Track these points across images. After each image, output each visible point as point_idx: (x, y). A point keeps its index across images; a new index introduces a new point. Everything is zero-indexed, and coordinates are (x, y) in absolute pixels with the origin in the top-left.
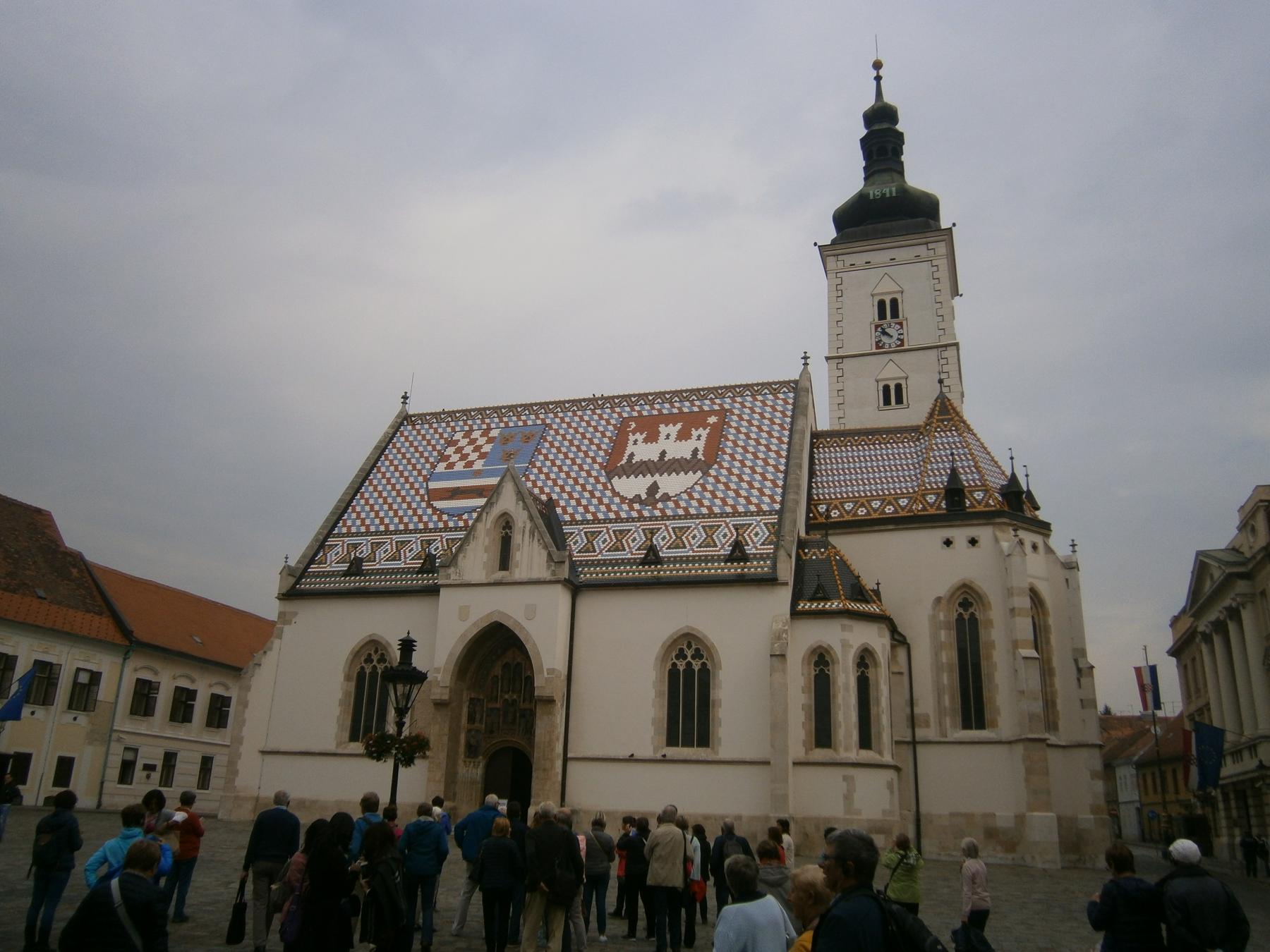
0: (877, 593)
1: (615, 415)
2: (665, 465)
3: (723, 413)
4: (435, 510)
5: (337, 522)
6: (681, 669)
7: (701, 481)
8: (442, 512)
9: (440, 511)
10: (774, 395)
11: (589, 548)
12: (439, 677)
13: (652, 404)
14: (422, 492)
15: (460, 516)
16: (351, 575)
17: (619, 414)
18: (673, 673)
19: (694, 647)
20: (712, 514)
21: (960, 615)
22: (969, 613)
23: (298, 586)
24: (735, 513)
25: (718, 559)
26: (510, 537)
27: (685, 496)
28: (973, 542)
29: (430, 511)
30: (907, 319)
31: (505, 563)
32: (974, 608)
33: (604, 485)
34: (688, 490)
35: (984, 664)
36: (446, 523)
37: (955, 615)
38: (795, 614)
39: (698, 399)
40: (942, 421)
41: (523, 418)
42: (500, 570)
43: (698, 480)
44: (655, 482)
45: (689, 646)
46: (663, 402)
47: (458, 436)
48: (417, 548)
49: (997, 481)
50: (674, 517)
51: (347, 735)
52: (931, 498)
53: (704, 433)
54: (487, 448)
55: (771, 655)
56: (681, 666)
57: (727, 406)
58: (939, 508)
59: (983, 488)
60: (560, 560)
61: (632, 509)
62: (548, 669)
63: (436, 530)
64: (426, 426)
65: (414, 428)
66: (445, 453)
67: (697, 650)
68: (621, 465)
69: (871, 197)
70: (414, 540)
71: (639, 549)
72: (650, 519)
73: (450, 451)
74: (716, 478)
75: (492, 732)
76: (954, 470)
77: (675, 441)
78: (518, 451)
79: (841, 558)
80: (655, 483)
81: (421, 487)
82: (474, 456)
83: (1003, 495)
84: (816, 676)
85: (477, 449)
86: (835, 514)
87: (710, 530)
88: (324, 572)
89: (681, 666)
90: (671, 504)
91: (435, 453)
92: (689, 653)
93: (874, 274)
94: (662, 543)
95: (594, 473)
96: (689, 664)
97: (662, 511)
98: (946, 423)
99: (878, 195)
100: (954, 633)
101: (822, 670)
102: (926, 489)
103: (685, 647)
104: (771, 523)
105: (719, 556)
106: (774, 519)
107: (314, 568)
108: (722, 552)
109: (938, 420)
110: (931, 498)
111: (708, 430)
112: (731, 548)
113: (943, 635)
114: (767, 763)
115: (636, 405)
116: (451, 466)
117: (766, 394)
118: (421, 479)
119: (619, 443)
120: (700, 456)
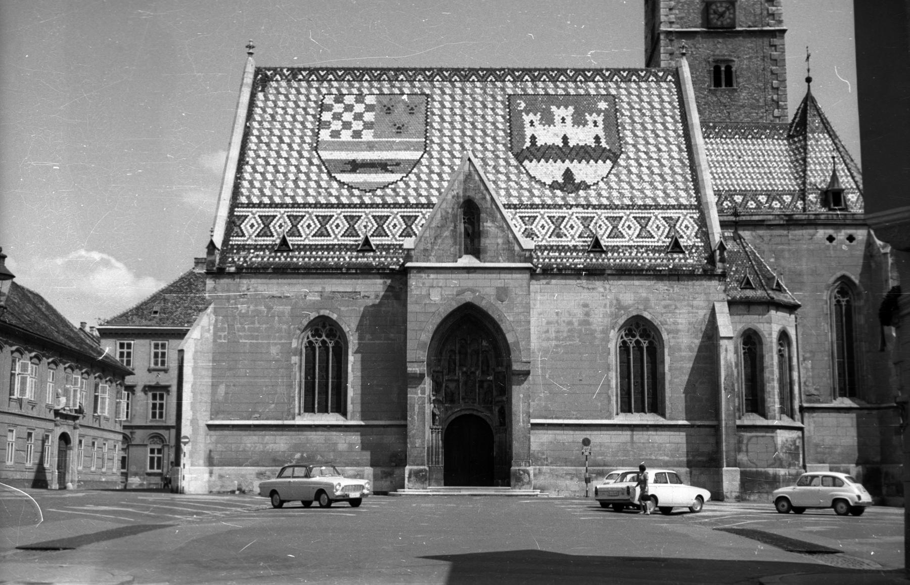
3: (612, 100)
4: (342, 184)
6: (631, 346)
8: (350, 187)
9: (348, 185)
14: (316, 161)
27: (601, 184)
29: (335, 184)
33: (517, 167)
43: (611, 170)
44: (568, 168)
47: (329, 100)
53: (600, 120)
54: (369, 117)
57: (613, 92)
63: (355, 206)
67: (645, 330)
68: (527, 148)
70: (336, 216)
73: (326, 116)
77: (573, 126)
80: (568, 170)
90: (592, 193)
91: (310, 118)
94: (601, 232)
97: (586, 198)
103: (633, 327)
112: (670, 240)
116: (336, 134)
120: (604, 144)
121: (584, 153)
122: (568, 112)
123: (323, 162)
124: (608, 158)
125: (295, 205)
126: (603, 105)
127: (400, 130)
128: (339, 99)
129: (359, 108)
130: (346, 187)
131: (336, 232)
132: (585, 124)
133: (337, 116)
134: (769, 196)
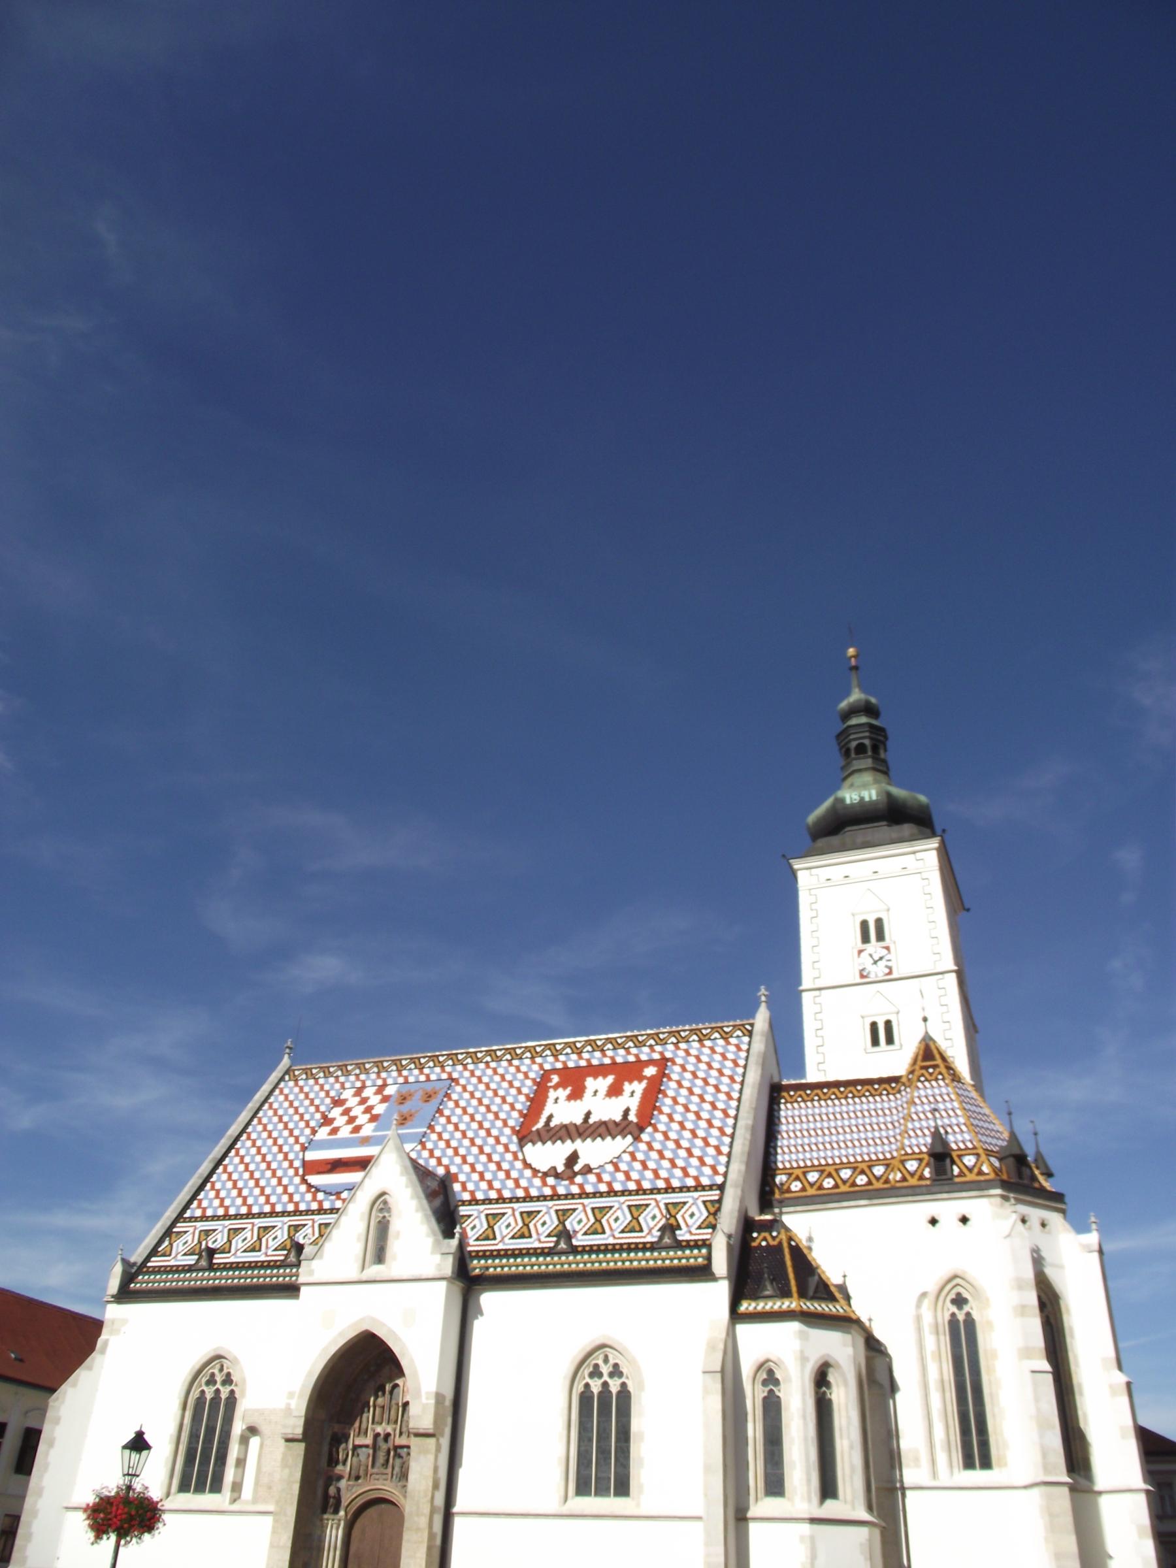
0: (843, 1288)
1: (536, 1067)
2: (589, 1129)
5: (190, 1202)
7: (631, 1149)
8: (318, 1190)
9: (316, 1188)
10: (726, 1039)
11: (489, 1235)
12: (293, 1406)
13: (579, 1053)
14: (297, 1164)
15: (338, 1194)
16: (198, 1270)
17: (541, 1066)
18: (586, 1398)
19: (612, 1361)
21: (953, 1315)
22: (964, 1311)
23: (132, 1285)
24: (669, 1189)
26: (388, 1221)
27: (610, 1168)
28: (964, 1220)
29: (303, 1188)
30: (895, 943)
31: (380, 1257)
32: (969, 1305)
34: (615, 1160)
36: (320, 1203)
37: (947, 1317)
39: (636, 1046)
40: (926, 1068)
41: (426, 1071)
42: (375, 1263)
43: (628, 1148)
45: (606, 1360)
46: (594, 1050)
47: (347, 1094)
49: (994, 1141)
50: (595, 1194)
54: (380, 1109)
55: (704, 1372)
56: (596, 1386)
57: (668, 1055)
58: (922, 1178)
59: (974, 1151)
60: (447, 1251)
61: (545, 1184)
62: (427, 1393)
63: (308, 1212)
64: (311, 1082)
65: (296, 1085)
66: (330, 1116)
68: (538, 1130)
69: (848, 801)
71: (549, 1235)
72: (566, 1197)
73: (336, 1113)
74: (649, 1145)
75: (357, 1478)
76: (936, 1128)
77: (604, 1099)
78: (417, 1112)
79: (797, 1245)
81: (297, 1157)
82: (363, 1119)
83: (1000, 1160)
84: (765, 1399)
85: (368, 1110)
86: (796, 1186)
87: (636, 1210)
88: (167, 1266)
89: (596, 1386)
91: (318, 1116)
92: (605, 1369)
95: (503, 1140)
96: (605, 1384)
97: (581, 1186)
98: (931, 1070)
99: (855, 800)
100: (946, 1340)
101: (771, 1391)
102: (907, 1154)
103: (600, 1362)
104: (711, 1201)
105: (644, 1244)
106: (714, 1195)
107: (155, 1262)
108: (649, 1239)
109: (922, 1068)
110: (912, 1165)
111: (644, 1084)
113: (930, 1342)
114: (699, 1518)
115: (561, 1054)
116: (335, 1131)
117: (716, 1039)
118: (297, 1148)
119: (537, 1101)
120: (632, 1117)
121: (606, 1129)
123: (305, 1163)
124: (630, 1133)
130: (313, 1190)
131: (270, 1245)
134: (855, 1169)
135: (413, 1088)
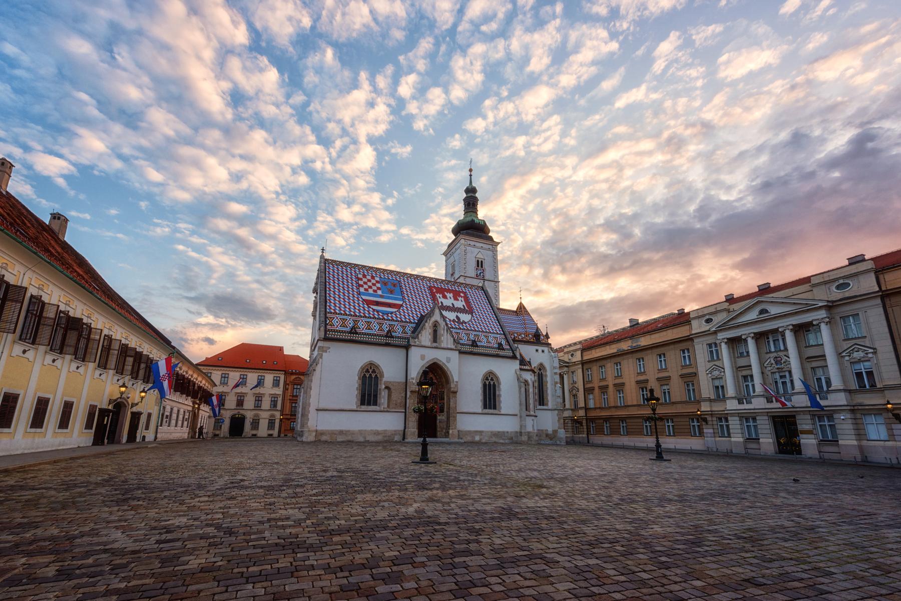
2: (452, 309)
4: (374, 310)
8: (378, 312)
15: (387, 314)
16: (353, 333)
18: (485, 385)
20: (483, 331)
25: (495, 348)
28: (543, 351)
35: (544, 387)
38: (521, 369)
47: (360, 276)
48: (377, 327)
51: (359, 403)
52: (531, 336)
54: (378, 285)
93: (476, 250)
107: (329, 327)
121: (458, 310)
122: (451, 295)
123: (364, 300)
125: (356, 316)
126: (462, 295)
127: (391, 292)
128: (364, 276)
129: (373, 281)
132: (458, 300)
133: (365, 283)
135: (386, 281)
